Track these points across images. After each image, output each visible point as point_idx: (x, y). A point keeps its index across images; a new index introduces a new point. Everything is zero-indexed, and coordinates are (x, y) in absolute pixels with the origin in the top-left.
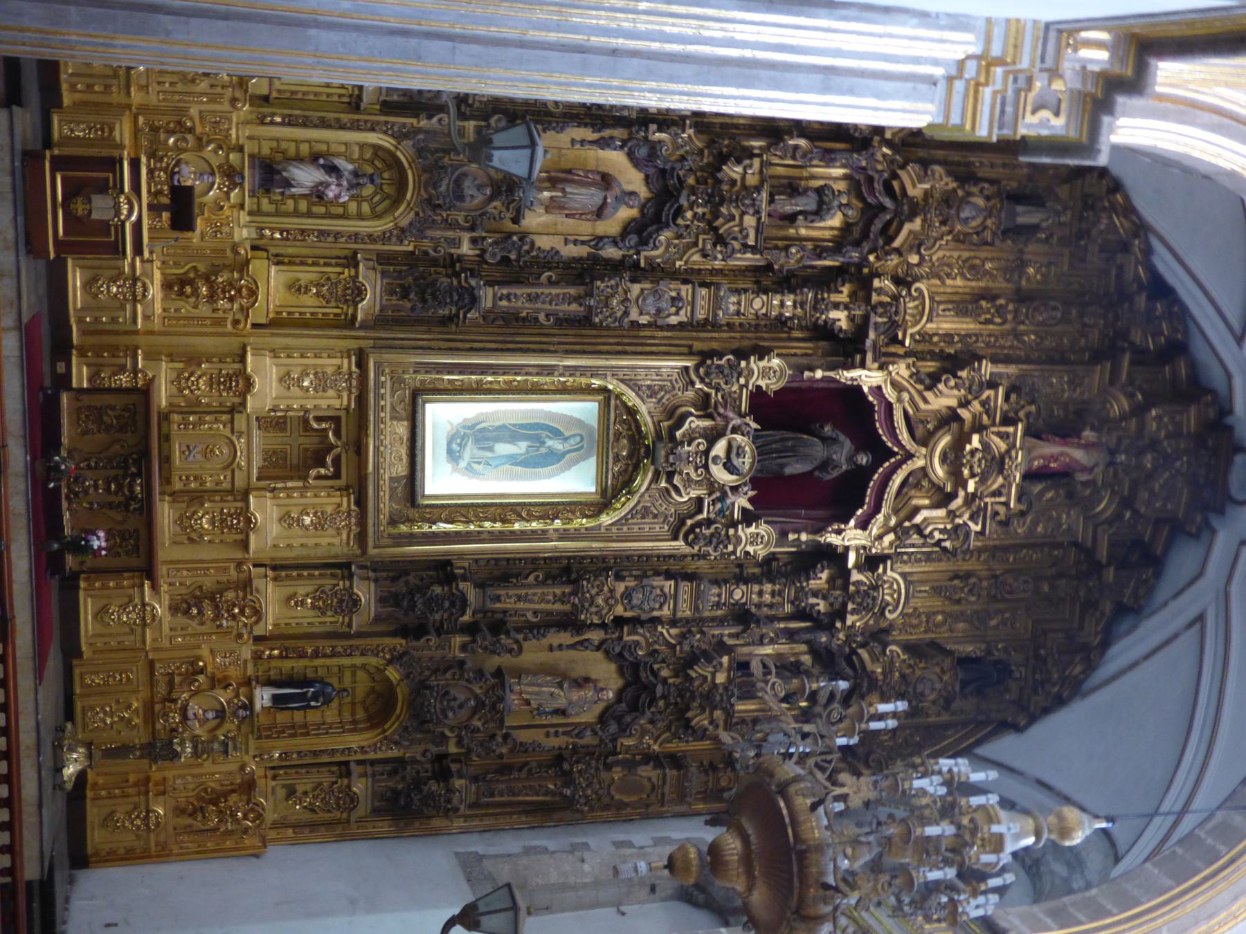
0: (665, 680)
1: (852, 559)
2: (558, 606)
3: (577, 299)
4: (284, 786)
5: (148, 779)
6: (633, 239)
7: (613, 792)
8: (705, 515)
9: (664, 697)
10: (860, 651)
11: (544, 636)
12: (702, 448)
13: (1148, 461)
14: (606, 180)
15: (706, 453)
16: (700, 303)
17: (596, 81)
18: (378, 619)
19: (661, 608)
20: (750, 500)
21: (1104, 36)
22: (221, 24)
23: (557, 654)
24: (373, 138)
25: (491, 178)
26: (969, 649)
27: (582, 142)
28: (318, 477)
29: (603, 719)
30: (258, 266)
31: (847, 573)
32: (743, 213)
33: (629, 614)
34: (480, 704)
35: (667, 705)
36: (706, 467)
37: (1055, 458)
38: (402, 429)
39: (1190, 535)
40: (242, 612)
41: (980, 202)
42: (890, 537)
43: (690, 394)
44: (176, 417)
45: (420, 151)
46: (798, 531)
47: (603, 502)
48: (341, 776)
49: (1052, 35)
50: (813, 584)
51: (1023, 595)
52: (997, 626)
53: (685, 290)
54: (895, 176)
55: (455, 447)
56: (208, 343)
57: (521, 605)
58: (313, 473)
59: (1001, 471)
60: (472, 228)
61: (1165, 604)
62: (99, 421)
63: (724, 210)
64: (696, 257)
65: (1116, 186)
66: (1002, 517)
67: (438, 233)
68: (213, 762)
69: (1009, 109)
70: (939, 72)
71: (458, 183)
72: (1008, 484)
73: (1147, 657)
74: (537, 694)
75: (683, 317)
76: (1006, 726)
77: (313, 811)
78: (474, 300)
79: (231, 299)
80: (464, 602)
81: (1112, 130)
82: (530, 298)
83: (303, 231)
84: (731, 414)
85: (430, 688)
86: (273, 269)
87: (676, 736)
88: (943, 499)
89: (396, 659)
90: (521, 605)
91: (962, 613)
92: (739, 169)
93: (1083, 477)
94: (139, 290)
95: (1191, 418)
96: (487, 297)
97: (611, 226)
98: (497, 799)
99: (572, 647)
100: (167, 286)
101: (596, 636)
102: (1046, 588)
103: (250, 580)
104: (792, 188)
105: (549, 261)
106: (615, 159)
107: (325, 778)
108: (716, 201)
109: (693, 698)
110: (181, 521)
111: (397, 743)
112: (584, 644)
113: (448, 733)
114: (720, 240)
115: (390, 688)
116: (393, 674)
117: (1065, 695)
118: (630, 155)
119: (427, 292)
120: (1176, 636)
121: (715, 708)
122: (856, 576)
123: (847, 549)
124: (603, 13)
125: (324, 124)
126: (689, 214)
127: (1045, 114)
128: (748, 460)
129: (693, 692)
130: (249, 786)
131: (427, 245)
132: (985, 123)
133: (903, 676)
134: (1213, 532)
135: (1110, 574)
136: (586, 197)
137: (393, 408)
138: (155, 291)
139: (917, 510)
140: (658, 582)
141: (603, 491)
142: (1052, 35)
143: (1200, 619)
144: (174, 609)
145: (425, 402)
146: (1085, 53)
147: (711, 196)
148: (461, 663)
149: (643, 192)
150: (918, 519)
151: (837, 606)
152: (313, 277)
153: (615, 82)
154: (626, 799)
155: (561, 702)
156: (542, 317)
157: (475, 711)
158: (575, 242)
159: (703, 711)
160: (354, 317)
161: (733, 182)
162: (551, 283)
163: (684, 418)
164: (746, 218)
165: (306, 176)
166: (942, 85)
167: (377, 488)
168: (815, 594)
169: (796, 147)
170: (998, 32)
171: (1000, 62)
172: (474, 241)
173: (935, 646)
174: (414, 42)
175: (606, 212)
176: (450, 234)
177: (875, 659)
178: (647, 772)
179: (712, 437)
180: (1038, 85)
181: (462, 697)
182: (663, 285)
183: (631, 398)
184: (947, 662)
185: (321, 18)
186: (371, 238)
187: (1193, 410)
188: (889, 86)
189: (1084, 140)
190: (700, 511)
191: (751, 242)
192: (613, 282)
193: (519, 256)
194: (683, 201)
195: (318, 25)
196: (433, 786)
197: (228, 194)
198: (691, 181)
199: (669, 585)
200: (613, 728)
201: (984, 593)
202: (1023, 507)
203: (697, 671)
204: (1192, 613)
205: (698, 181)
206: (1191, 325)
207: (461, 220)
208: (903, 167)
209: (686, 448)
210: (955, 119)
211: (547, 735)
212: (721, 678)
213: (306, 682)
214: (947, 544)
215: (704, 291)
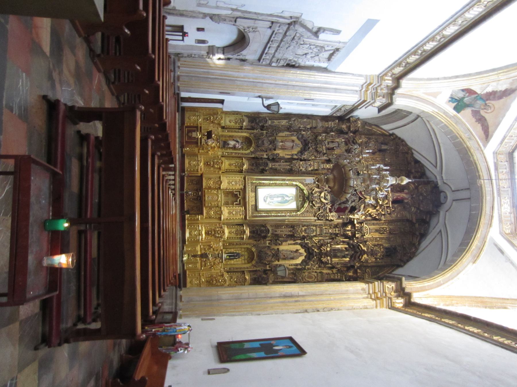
0: (315, 252)
1: (355, 222)
2: (290, 233)
3: (289, 165)
4: (230, 276)
5: (200, 274)
6: (300, 154)
7: (306, 278)
8: (321, 212)
9: (316, 256)
10: (361, 245)
11: (287, 241)
12: (319, 195)
13: (421, 198)
14: (293, 141)
15: (320, 196)
16: (315, 166)
17: (290, 91)
18: (250, 238)
19: (313, 233)
20: (331, 206)
21: (390, 78)
22: (220, 80)
23: (290, 246)
24: (245, 134)
25: (269, 140)
26: (386, 245)
27: (288, 135)
28: (236, 204)
29: (302, 262)
30: (223, 159)
31: (355, 225)
32: (323, 146)
33: (306, 235)
34: (274, 255)
35: (317, 258)
36: (320, 199)
37: (399, 196)
38: (253, 194)
39: (434, 214)
40: (220, 232)
41: (373, 142)
42: (364, 217)
43: (315, 185)
44: (206, 191)
45: (255, 136)
46: (342, 216)
47: (298, 210)
48: (242, 274)
49: (379, 78)
50: (347, 229)
51: (397, 232)
52: (392, 241)
53: (312, 163)
54: (354, 139)
55: (265, 199)
56: (212, 176)
57: (281, 233)
58: (235, 203)
59: (387, 199)
60: (266, 152)
61: (432, 231)
62: (192, 183)
63: (318, 146)
64: (313, 158)
65: (403, 141)
66: (389, 212)
67: (258, 153)
68: (214, 270)
69: (373, 96)
70: (358, 89)
71: (263, 141)
72: (389, 201)
73: (429, 244)
74: (286, 253)
75: (312, 168)
76: (399, 266)
77: (237, 282)
78: (267, 164)
79: (218, 165)
80: (269, 230)
81: (395, 101)
82: (279, 165)
83: (231, 153)
84: (324, 187)
85: (262, 252)
86: (226, 160)
87: (320, 267)
88: (374, 207)
89: (254, 246)
90: (281, 233)
91: (384, 237)
92: (321, 137)
93: (406, 201)
94: (199, 163)
95: (429, 188)
96: (270, 165)
97: (295, 152)
98: (279, 280)
99: (293, 244)
100: (204, 164)
101: (299, 242)
102: (402, 230)
103: (222, 227)
104: (332, 142)
105: (283, 158)
106: (294, 138)
107: (239, 274)
108: (316, 144)
109: (322, 255)
110: (208, 213)
111: (255, 266)
112: (296, 244)
113: (267, 263)
114: (317, 151)
115: (253, 253)
116: (254, 250)
117: (412, 256)
118: (298, 138)
119: (257, 165)
120: (436, 237)
121: (327, 257)
122: (357, 225)
123: (354, 219)
124: (291, 74)
125: (235, 132)
126: (311, 148)
127: (381, 97)
128: (329, 197)
129: (322, 253)
130: (222, 275)
131: (257, 156)
132: (369, 98)
133: (372, 250)
134: (439, 212)
135: (417, 225)
136: (289, 144)
137: (251, 190)
138: (202, 164)
139: (369, 211)
140: (312, 227)
141: (297, 207)
142: (379, 78)
143: (440, 231)
144: (206, 233)
145: (258, 188)
146: (387, 81)
147: (315, 144)
148: (269, 247)
149: (301, 146)
150: (369, 212)
151: (353, 233)
152: (234, 162)
153: (293, 91)
154: (309, 280)
155: (291, 256)
156: (282, 170)
157: (273, 257)
158: (288, 155)
159: (325, 258)
160: (243, 170)
161: (320, 140)
162: (283, 162)
163: (313, 190)
164: (323, 147)
165: (232, 143)
166: (359, 92)
167: (249, 207)
168: (348, 231)
169: (332, 135)
170: (368, 78)
171: (370, 84)
172: (267, 155)
173: (378, 245)
174: (255, 83)
175: (294, 147)
176: (261, 153)
177: (364, 246)
178: (314, 274)
179: (321, 193)
180: (379, 91)
181: (270, 253)
182: (307, 162)
183: (302, 186)
184: (381, 247)
185: (238, 79)
186: (246, 154)
187: (429, 186)
188: (348, 92)
189: (390, 102)
190: (320, 211)
191: (325, 152)
192: (296, 161)
193: (276, 157)
194: (310, 146)
195: (237, 80)
196: (264, 276)
197: (217, 145)
198: (311, 141)
199: (314, 228)
200: (304, 264)
201: (388, 232)
202: (393, 210)
203: (323, 248)
204: (438, 231)
205: (312, 141)
206: (425, 169)
207: (264, 149)
208: (356, 137)
209: (315, 195)
210: (363, 99)
211: (290, 265)
212: (328, 249)
213: (233, 253)
214: (377, 217)
215: (316, 163)
